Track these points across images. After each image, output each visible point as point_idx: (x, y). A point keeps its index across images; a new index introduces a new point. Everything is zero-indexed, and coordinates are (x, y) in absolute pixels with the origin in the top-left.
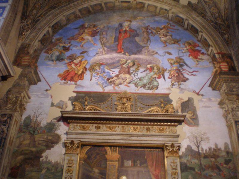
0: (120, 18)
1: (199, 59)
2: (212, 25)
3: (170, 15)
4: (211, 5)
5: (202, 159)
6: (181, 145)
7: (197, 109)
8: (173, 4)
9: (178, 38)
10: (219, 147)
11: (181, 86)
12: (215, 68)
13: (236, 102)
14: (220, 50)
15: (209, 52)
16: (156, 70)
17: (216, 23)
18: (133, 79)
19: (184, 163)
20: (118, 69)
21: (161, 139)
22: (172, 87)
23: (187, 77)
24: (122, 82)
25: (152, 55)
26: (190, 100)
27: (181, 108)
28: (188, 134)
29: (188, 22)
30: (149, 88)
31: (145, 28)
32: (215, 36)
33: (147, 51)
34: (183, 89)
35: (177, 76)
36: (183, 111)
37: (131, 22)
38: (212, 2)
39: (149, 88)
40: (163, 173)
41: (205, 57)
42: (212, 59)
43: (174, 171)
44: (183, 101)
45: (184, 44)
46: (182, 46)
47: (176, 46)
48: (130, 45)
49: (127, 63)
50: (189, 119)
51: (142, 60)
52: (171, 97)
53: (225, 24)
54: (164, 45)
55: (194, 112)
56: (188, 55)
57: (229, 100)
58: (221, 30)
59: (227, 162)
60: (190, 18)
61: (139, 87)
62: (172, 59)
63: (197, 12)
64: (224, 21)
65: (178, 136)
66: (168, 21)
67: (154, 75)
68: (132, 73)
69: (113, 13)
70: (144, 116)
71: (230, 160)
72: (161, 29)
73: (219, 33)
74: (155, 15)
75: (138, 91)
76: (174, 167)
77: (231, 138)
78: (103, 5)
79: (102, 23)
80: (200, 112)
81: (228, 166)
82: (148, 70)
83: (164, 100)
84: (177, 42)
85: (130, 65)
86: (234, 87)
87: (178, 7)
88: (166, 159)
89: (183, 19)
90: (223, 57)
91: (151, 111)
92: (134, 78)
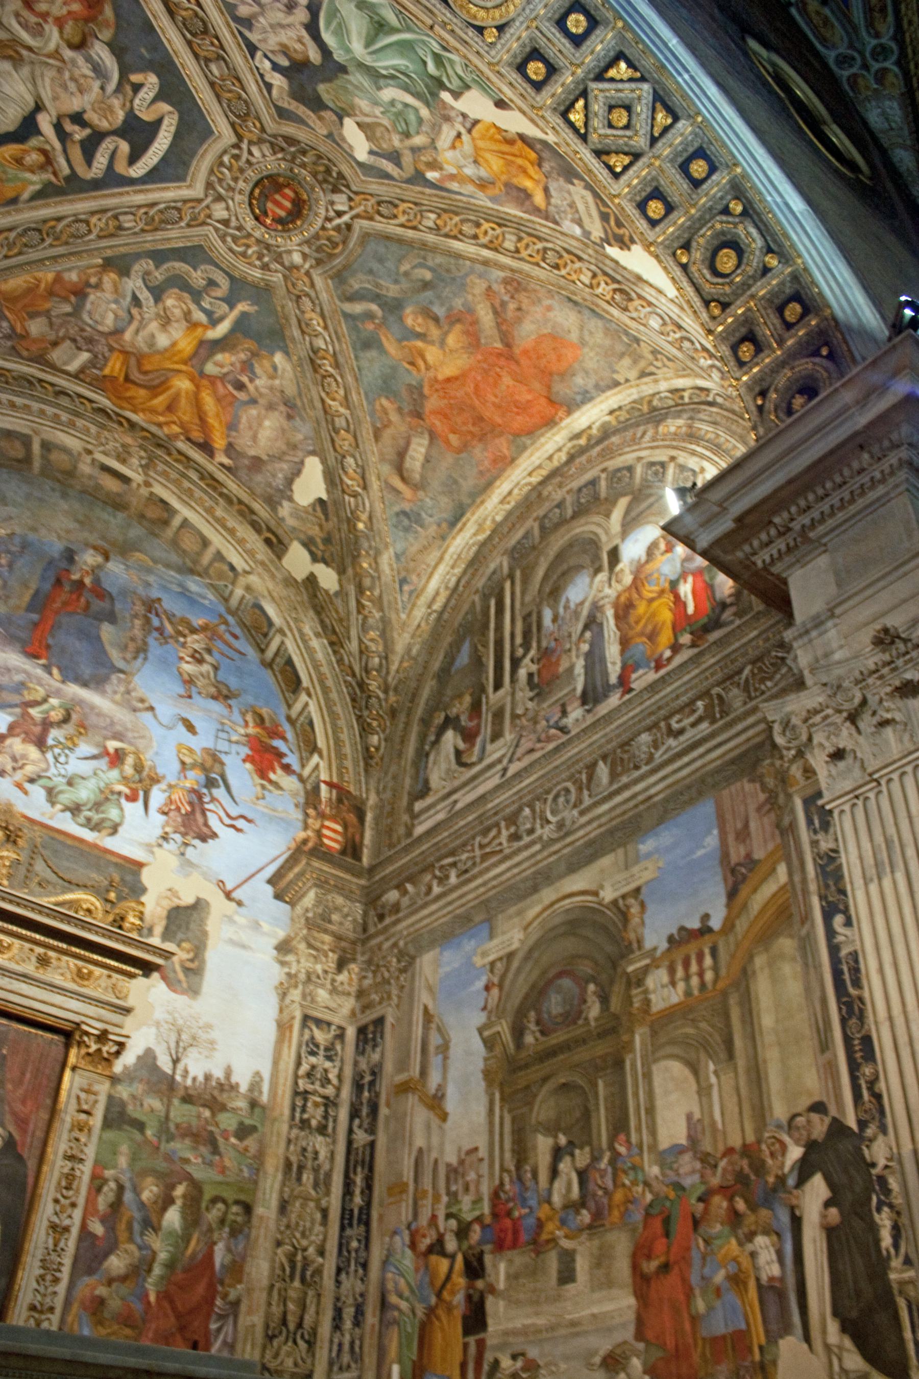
0: (77, 525)
1: (270, 781)
2: (348, 684)
3: (239, 592)
4: (371, 621)
5: (176, 1102)
6: (129, 1043)
7: (211, 943)
8: (259, 557)
9: (233, 682)
10: (234, 1079)
11: (189, 851)
12: (306, 827)
13: (326, 956)
14: (340, 775)
15: (306, 772)
16: (129, 770)
17: (362, 685)
18: (46, 770)
19: (121, 1100)
20: (10, 714)
21: (74, 1004)
22: (160, 846)
23: (215, 829)
24: (9, 768)
25: (135, 710)
26: (199, 906)
27: (164, 923)
28: (159, 1014)
29: (283, 643)
30: (89, 820)
31: (144, 603)
32: (342, 723)
33: (122, 689)
34: (190, 864)
35: (187, 814)
36: (167, 935)
37: (107, 558)
38: (377, 615)
39: (89, 820)
40: (45, 1116)
41: (289, 782)
42: (307, 799)
43: (83, 1116)
44: (177, 902)
45: (243, 714)
46: (237, 717)
47: (217, 707)
48: (77, 644)
49: (45, 707)
50: (178, 968)
51: (100, 715)
52: (146, 877)
53: (386, 700)
54: (182, 691)
55: (199, 951)
56: (243, 756)
57: (310, 946)
58: (366, 713)
59: (243, 1131)
60: (291, 630)
61: (59, 807)
62: (191, 750)
63: (322, 622)
64: (386, 691)
65: (127, 1011)
66: (222, 610)
67: (119, 782)
68: (52, 747)
69: (57, 494)
70: (48, 915)
71: (254, 1129)
72: (194, 631)
73: (359, 718)
74: (192, 572)
75: (51, 818)
76: (85, 1107)
77: (276, 1062)
78: (36, 447)
79: (11, 518)
80: (213, 956)
81: (241, 1145)
82: (107, 759)
83: (122, 880)
84: (227, 697)
85: (56, 715)
86: (337, 909)
87: (273, 576)
88: (68, 1074)
89: (270, 624)
90: (340, 800)
91: (70, 904)
92: (53, 771)
